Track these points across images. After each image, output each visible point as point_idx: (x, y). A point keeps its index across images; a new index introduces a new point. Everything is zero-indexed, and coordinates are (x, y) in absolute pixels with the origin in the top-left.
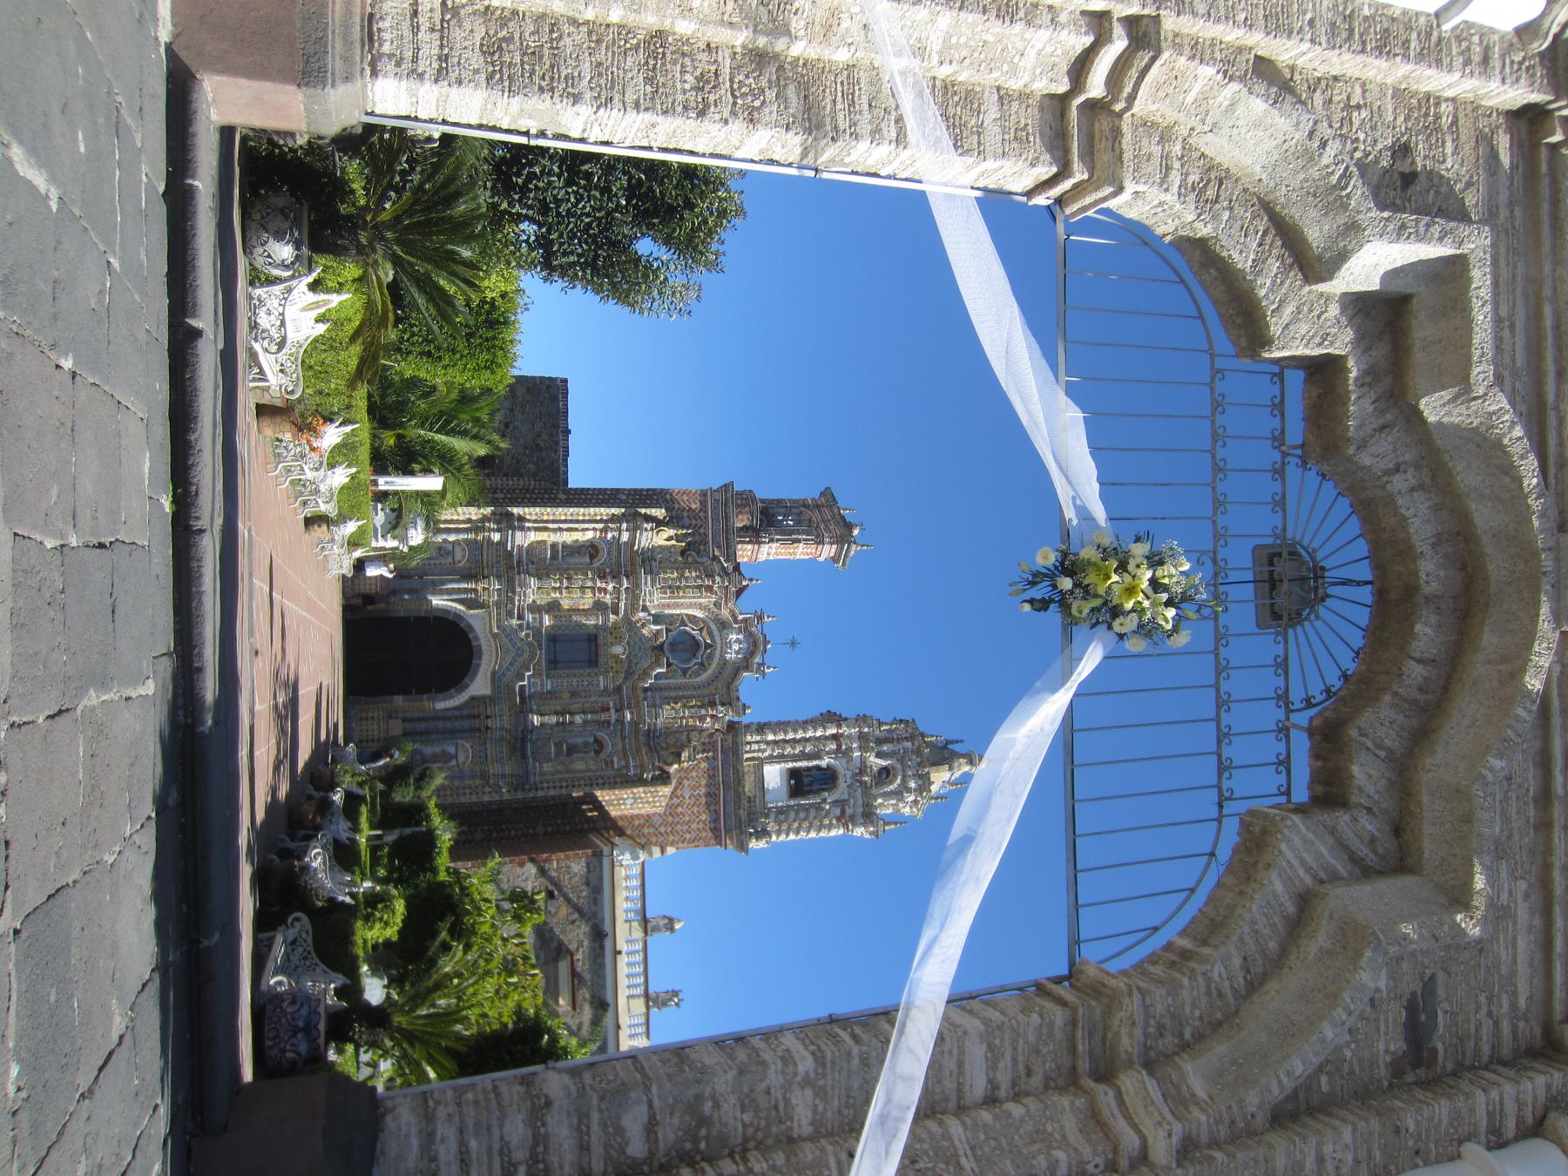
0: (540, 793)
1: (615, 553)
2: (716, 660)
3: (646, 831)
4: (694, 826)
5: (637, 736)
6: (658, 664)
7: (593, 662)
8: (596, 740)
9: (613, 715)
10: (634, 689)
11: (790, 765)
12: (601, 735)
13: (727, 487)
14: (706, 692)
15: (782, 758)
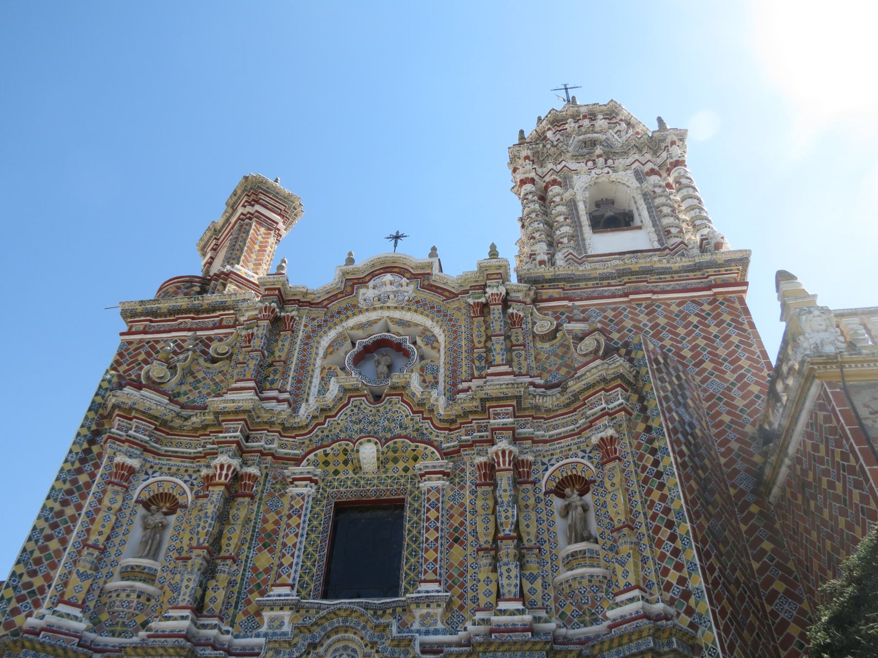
0: (697, 582)
1: (175, 462)
2: (408, 316)
3: (740, 403)
4: (714, 330)
5: (551, 414)
6: (400, 390)
7: (393, 508)
8: (559, 491)
9: (503, 444)
10: (450, 424)
11: (587, 230)
12: (545, 480)
13: (129, 314)
14: (463, 323)
15: (577, 237)
